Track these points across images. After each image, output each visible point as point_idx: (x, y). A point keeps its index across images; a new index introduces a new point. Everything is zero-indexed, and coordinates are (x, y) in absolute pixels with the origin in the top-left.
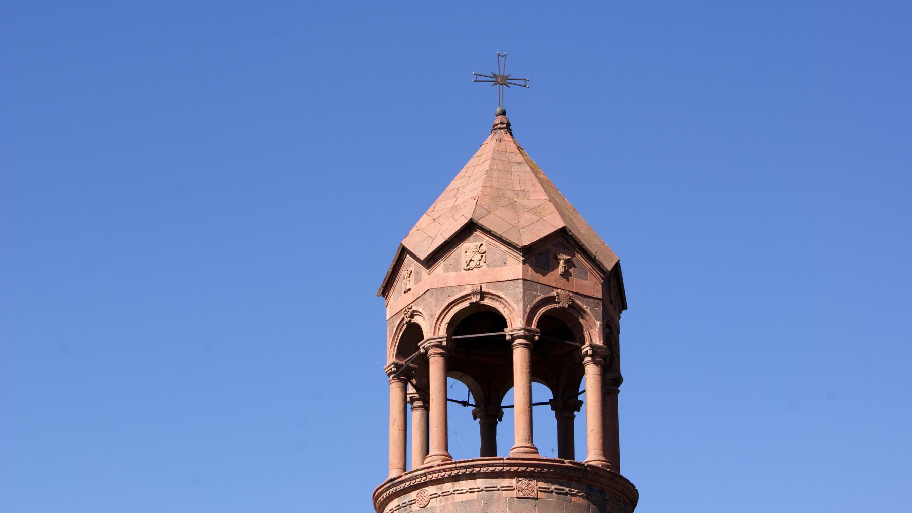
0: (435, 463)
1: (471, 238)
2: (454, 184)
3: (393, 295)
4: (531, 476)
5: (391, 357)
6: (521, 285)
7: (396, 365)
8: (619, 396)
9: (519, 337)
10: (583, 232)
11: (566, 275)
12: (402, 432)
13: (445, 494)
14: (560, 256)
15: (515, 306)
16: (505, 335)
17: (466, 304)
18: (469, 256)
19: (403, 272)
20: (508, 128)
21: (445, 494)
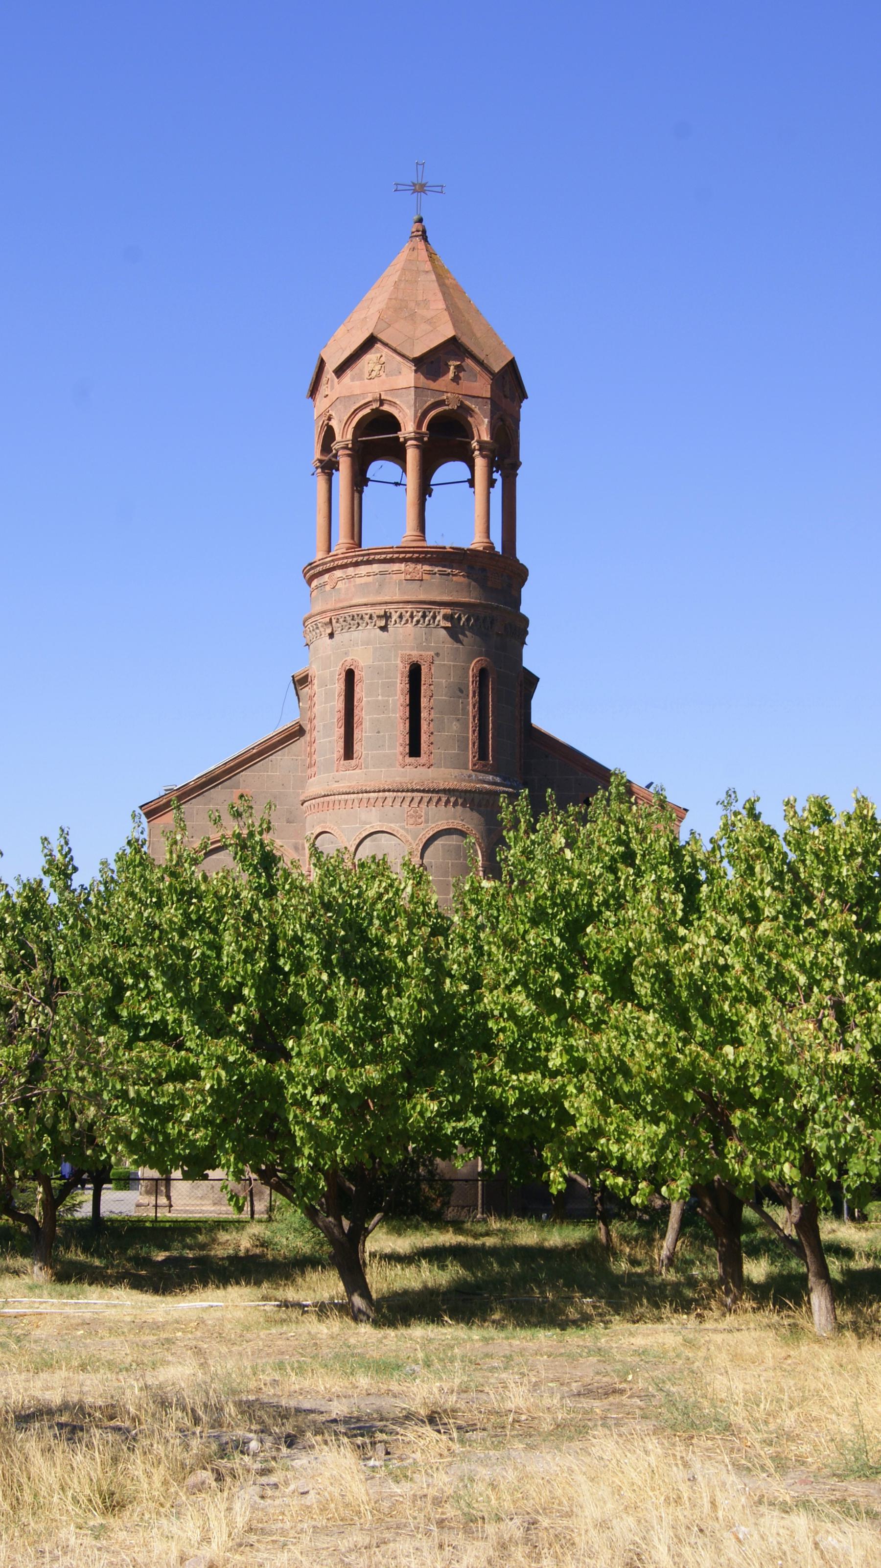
0: (339, 552)
1: (373, 350)
2: (369, 295)
3: (319, 396)
4: (417, 561)
5: (317, 455)
6: (413, 393)
7: (320, 461)
8: (518, 479)
9: (411, 439)
10: (479, 335)
11: (456, 379)
12: (326, 519)
13: (349, 578)
14: (451, 363)
15: (407, 411)
16: (398, 438)
17: (367, 411)
18: (371, 366)
19: (324, 380)
20: (424, 236)
21: (349, 578)
